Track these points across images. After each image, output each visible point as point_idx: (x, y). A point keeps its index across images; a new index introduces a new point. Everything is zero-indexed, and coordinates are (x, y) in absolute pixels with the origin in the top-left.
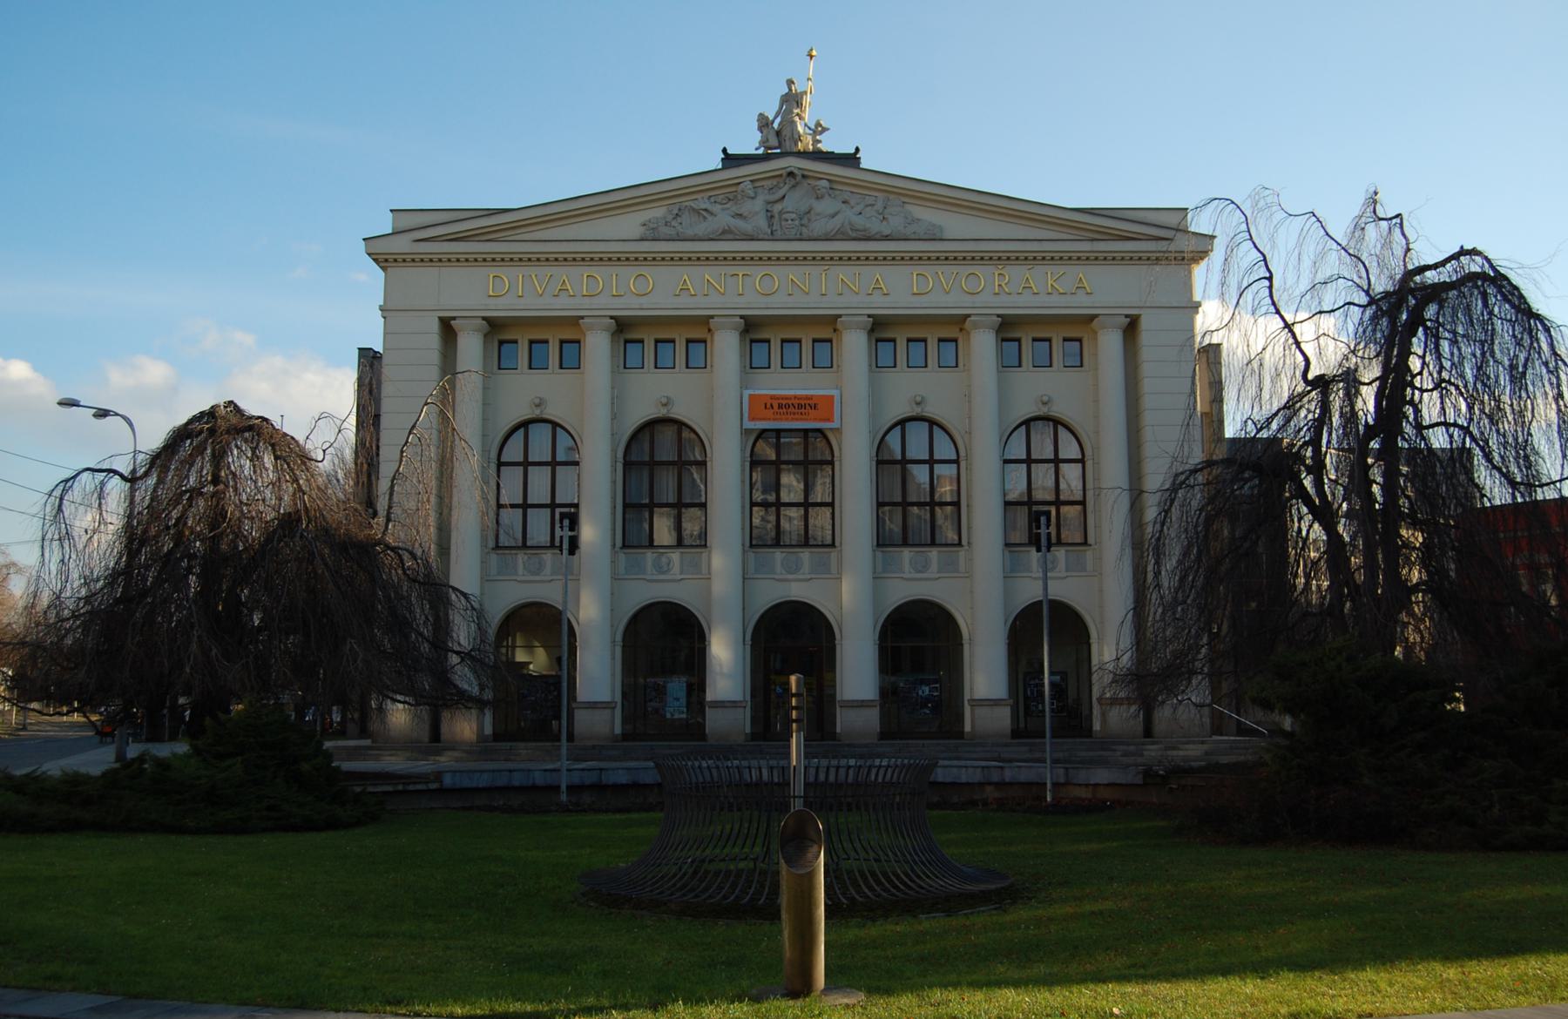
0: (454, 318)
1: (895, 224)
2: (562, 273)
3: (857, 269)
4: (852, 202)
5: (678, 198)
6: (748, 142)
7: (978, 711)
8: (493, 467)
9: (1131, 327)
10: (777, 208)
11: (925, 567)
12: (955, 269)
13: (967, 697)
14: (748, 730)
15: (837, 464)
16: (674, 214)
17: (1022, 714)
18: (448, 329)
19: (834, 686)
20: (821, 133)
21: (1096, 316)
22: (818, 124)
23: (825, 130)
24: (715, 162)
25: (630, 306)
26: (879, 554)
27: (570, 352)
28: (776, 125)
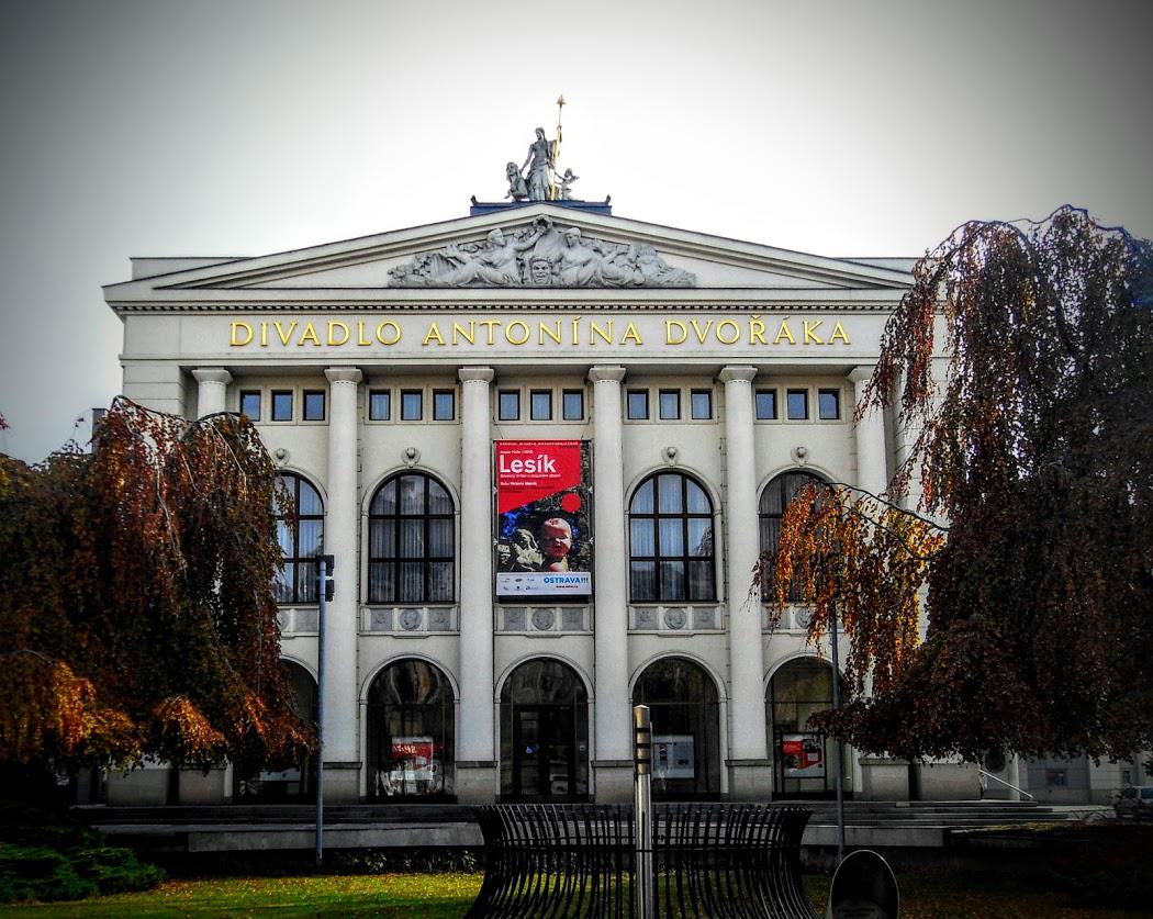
0: (196, 368)
1: (649, 272)
2: (308, 323)
3: (610, 319)
4: (604, 251)
5: (427, 246)
6: (497, 190)
10: (527, 256)
11: (680, 624)
12: (710, 319)
13: (724, 757)
14: (498, 793)
16: (422, 264)
19: (585, 738)
21: (856, 366)
22: (569, 172)
23: (574, 178)
25: (378, 356)
26: (632, 610)
27: (316, 407)
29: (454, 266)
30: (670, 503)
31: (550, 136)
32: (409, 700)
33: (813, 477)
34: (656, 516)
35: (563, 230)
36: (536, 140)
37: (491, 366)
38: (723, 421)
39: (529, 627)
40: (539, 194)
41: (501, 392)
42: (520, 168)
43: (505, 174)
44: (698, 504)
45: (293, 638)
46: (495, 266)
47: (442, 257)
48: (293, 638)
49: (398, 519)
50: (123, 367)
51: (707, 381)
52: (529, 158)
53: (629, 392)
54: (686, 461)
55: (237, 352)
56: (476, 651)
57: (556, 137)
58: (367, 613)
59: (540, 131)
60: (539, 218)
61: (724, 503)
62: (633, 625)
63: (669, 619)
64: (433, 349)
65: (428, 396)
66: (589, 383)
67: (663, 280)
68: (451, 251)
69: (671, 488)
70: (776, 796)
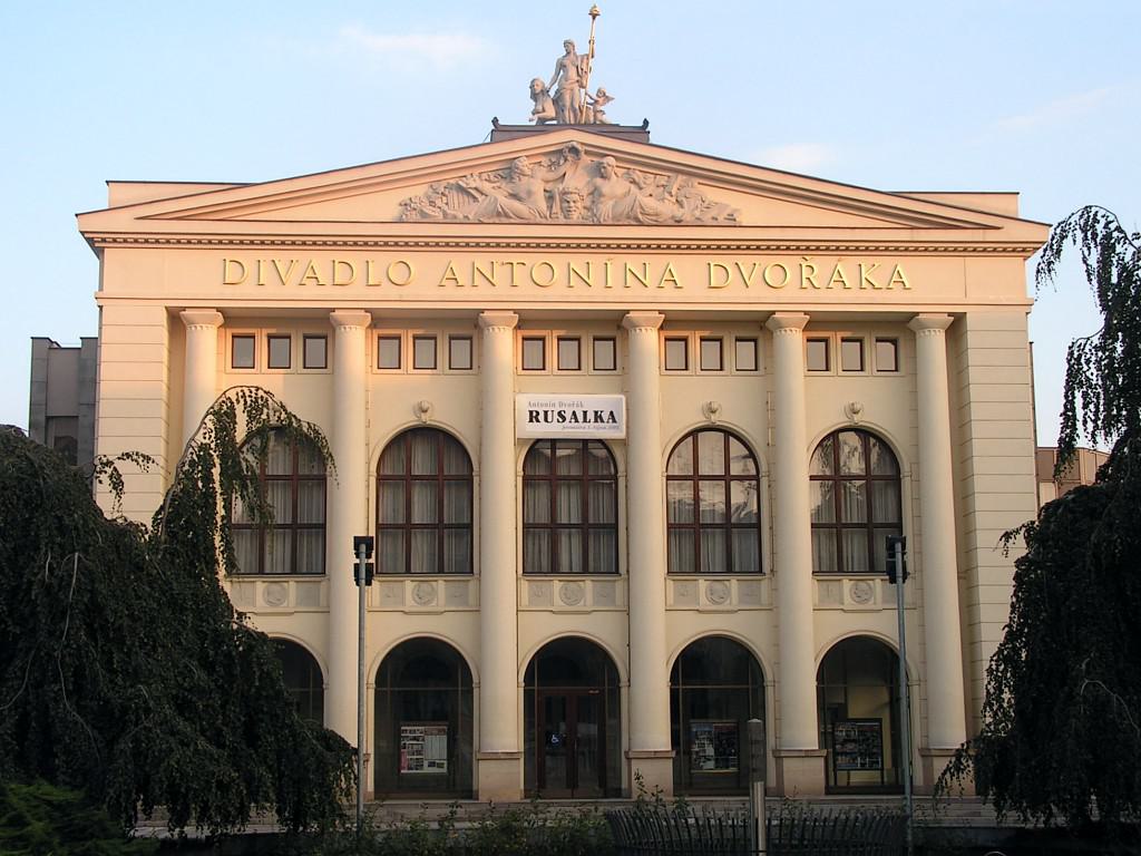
0: (184, 309)
5: (445, 177)
6: (520, 112)
9: (956, 328)
14: (522, 787)
17: (831, 769)
18: (177, 322)
21: (918, 313)
22: (601, 93)
23: (608, 99)
26: (670, 583)
28: (552, 93)
29: (474, 197)
31: (582, 49)
38: (914, 373)
39: (846, 602)
40: (569, 117)
46: (519, 199)
49: (408, 480)
50: (101, 307)
56: (508, 622)
58: (525, 585)
59: (568, 45)
60: (570, 145)
61: (772, 464)
62: (671, 601)
63: (712, 592)
64: (451, 292)
65: (552, 345)
66: (913, 335)
69: (711, 446)
70: (829, 790)
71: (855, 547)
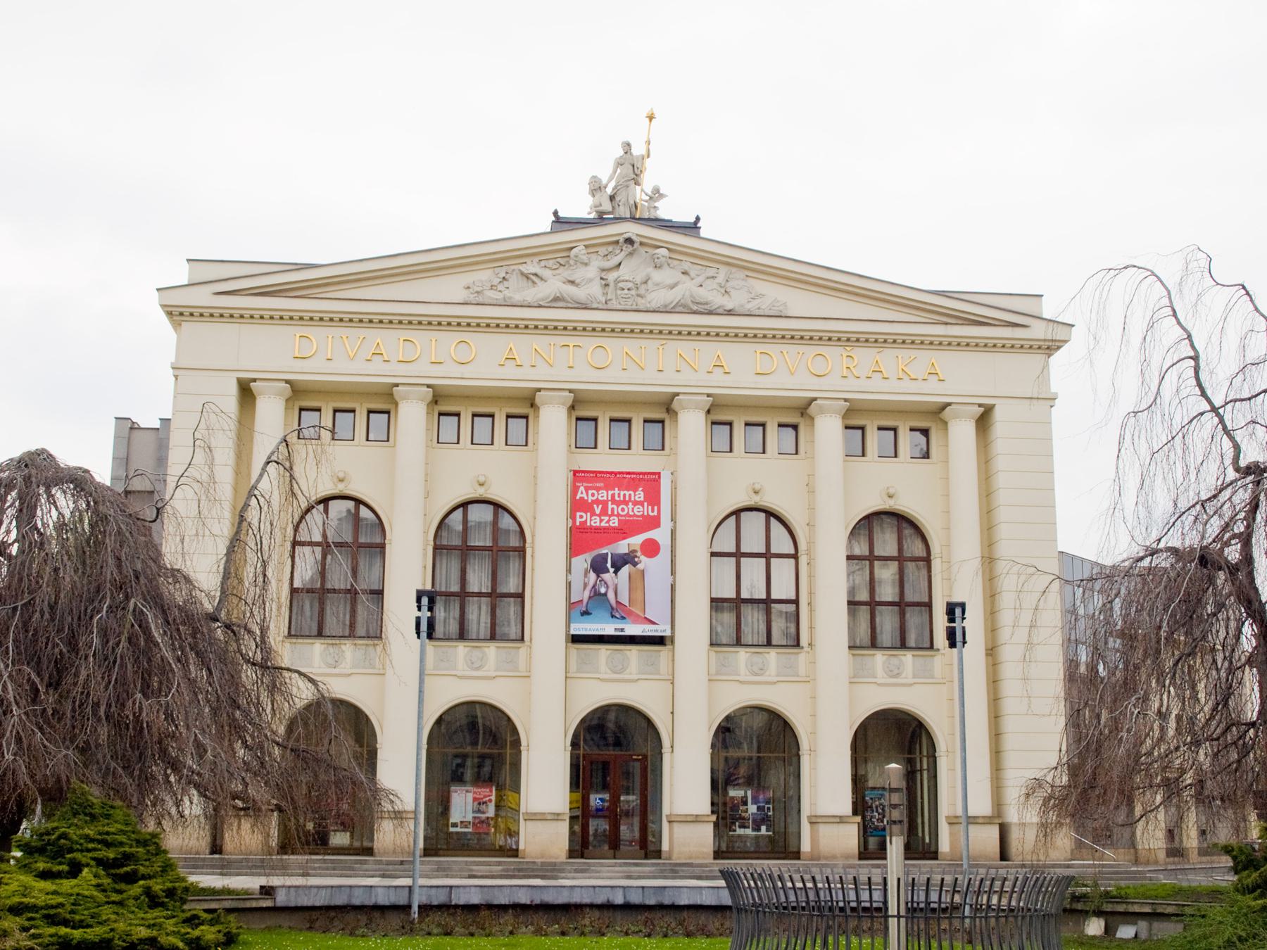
0: (254, 380)
4: (692, 274)
6: (582, 208)
7: (824, 830)
8: (288, 545)
9: (984, 420)
10: (612, 276)
11: (762, 671)
12: (801, 349)
13: (806, 811)
15: (936, 565)
18: (246, 392)
20: (657, 200)
21: (949, 404)
22: (657, 191)
23: (662, 196)
24: (546, 224)
25: (451, 375)
26: (713, 654)
29: (534, 282)
30: (754, 542)
31: (638, 150)
32: (474, 745)
33: (903, 522)
34: (738, 555)
35: (651, 251)
36: (622, 153)
37: (570, 391)
41: (578, 419)
42: (604, 182)
43: (587, 188)
44: (781, 542)
45: (911, 685)
46: (577, 285)
47: (522, 274)
48: (911, 685)
49: (465, 551)
50: (176, 377)
51: (797, 416)
52: (615, 172)
53: (713, 423)
54: (904, 504)
55: (299, 365)
57: (644, 152)
59: (627, 146)
60: (626, 236)
61: (810, 543)
62: (713, 671)
67: (751, 306)
68: (531, 267)
71: (887, 622)
